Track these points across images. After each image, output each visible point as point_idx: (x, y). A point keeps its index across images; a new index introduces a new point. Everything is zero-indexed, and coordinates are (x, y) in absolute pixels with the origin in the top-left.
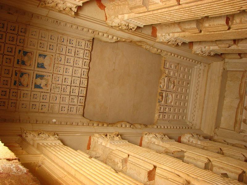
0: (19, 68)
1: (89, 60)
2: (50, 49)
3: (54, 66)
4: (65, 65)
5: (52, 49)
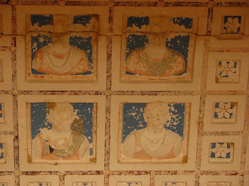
0: (111, 30)
2: (213, 145)
3: (139, 173)
5: (213, 155)
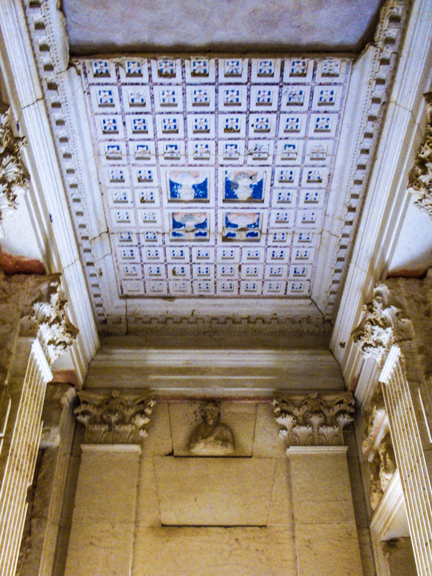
0: (216, 236)
1: (149, 62)
4: (186, 137)
